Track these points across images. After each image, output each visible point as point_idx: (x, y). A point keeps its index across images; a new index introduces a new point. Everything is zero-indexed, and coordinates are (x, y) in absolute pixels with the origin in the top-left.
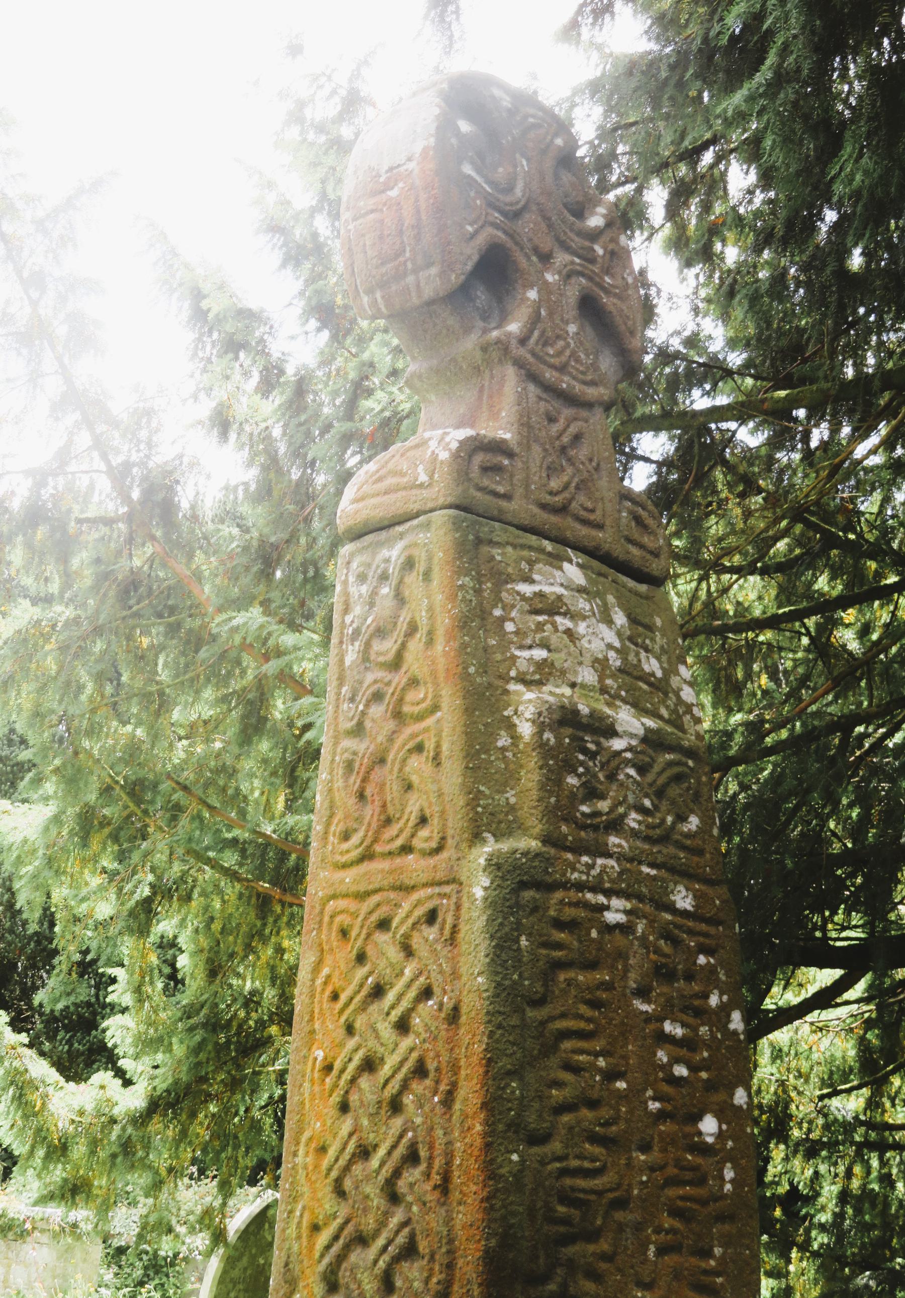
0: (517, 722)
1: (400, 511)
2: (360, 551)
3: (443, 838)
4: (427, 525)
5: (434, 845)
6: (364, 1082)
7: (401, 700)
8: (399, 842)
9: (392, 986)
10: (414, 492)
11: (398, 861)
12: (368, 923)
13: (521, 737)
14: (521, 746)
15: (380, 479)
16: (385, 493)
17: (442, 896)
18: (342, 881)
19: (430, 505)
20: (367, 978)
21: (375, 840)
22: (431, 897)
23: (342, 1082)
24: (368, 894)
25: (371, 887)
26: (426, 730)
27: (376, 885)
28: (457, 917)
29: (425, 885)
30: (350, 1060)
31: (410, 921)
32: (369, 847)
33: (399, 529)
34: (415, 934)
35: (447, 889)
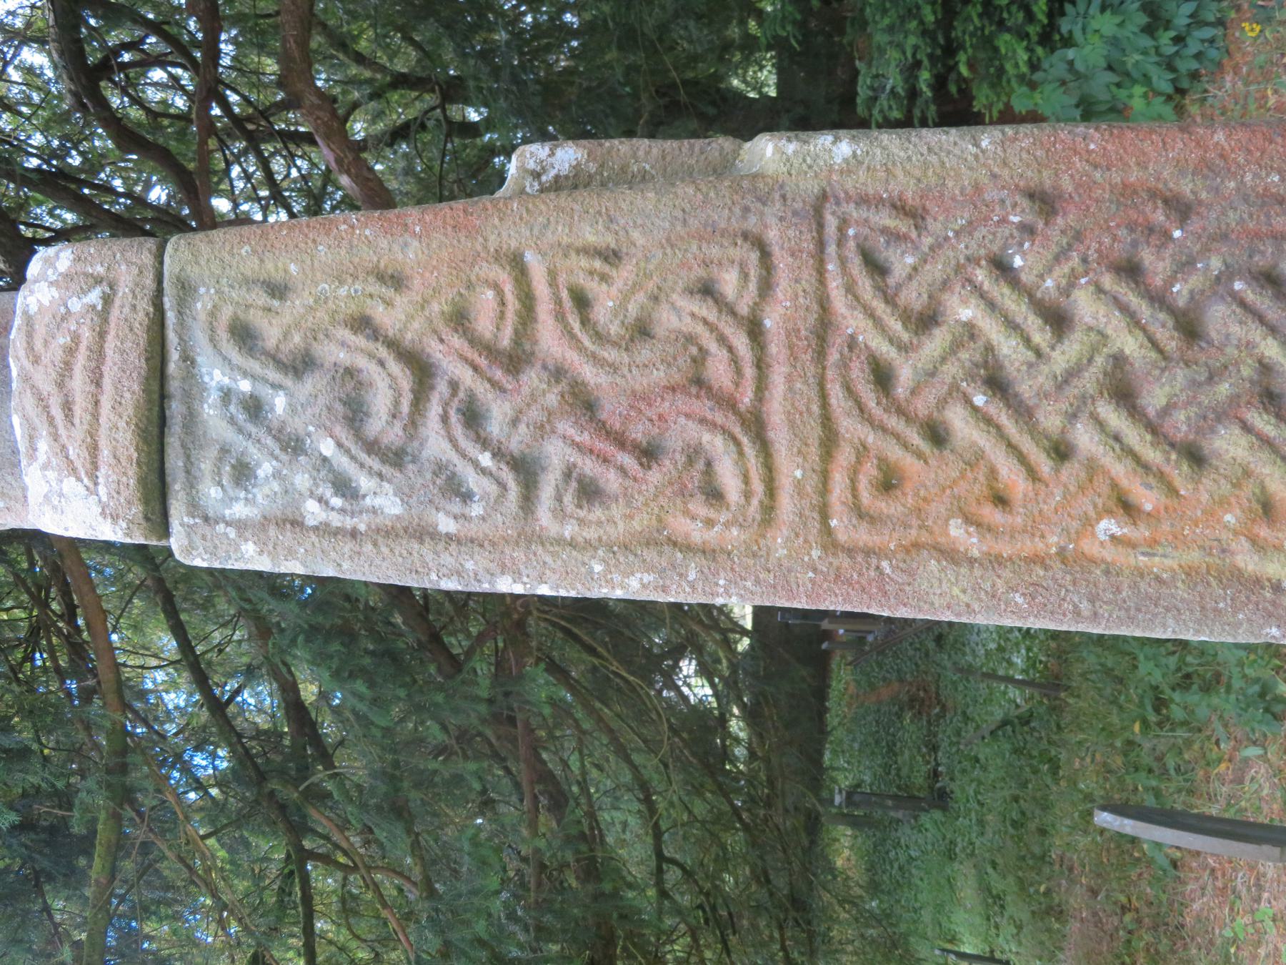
0: (552, 173)
1: (143, 338)
2: (192, 481)
3: (745, 236)
4: (186, 289)
5: (754, 256)
6: (1154, 398)
7: (489, 350)
8: (741, 342)
9: (989, 348)
10: (115, 313)
11: (775, 348)
12: (877, 412)
13: (577, 168)
14: (592, 167)
15: (67, 407)
16: (98, 384)
17: (844, 224)
18: (798, 485)
19: (149, 281)
20: (975, 409)
21: (728, 403)
22: (843, 262)
23: (1153, 455)
24: (827, 420)
25: (815, 408)
26: (552, 275)
27: (814, 394)
28: (879, 202)
29: (821, 272)
30: (1117, 438)
31: (880, 307)
32: (744, 423)
33: (174, 355)
34: (902, 300)
35: (831, 223)
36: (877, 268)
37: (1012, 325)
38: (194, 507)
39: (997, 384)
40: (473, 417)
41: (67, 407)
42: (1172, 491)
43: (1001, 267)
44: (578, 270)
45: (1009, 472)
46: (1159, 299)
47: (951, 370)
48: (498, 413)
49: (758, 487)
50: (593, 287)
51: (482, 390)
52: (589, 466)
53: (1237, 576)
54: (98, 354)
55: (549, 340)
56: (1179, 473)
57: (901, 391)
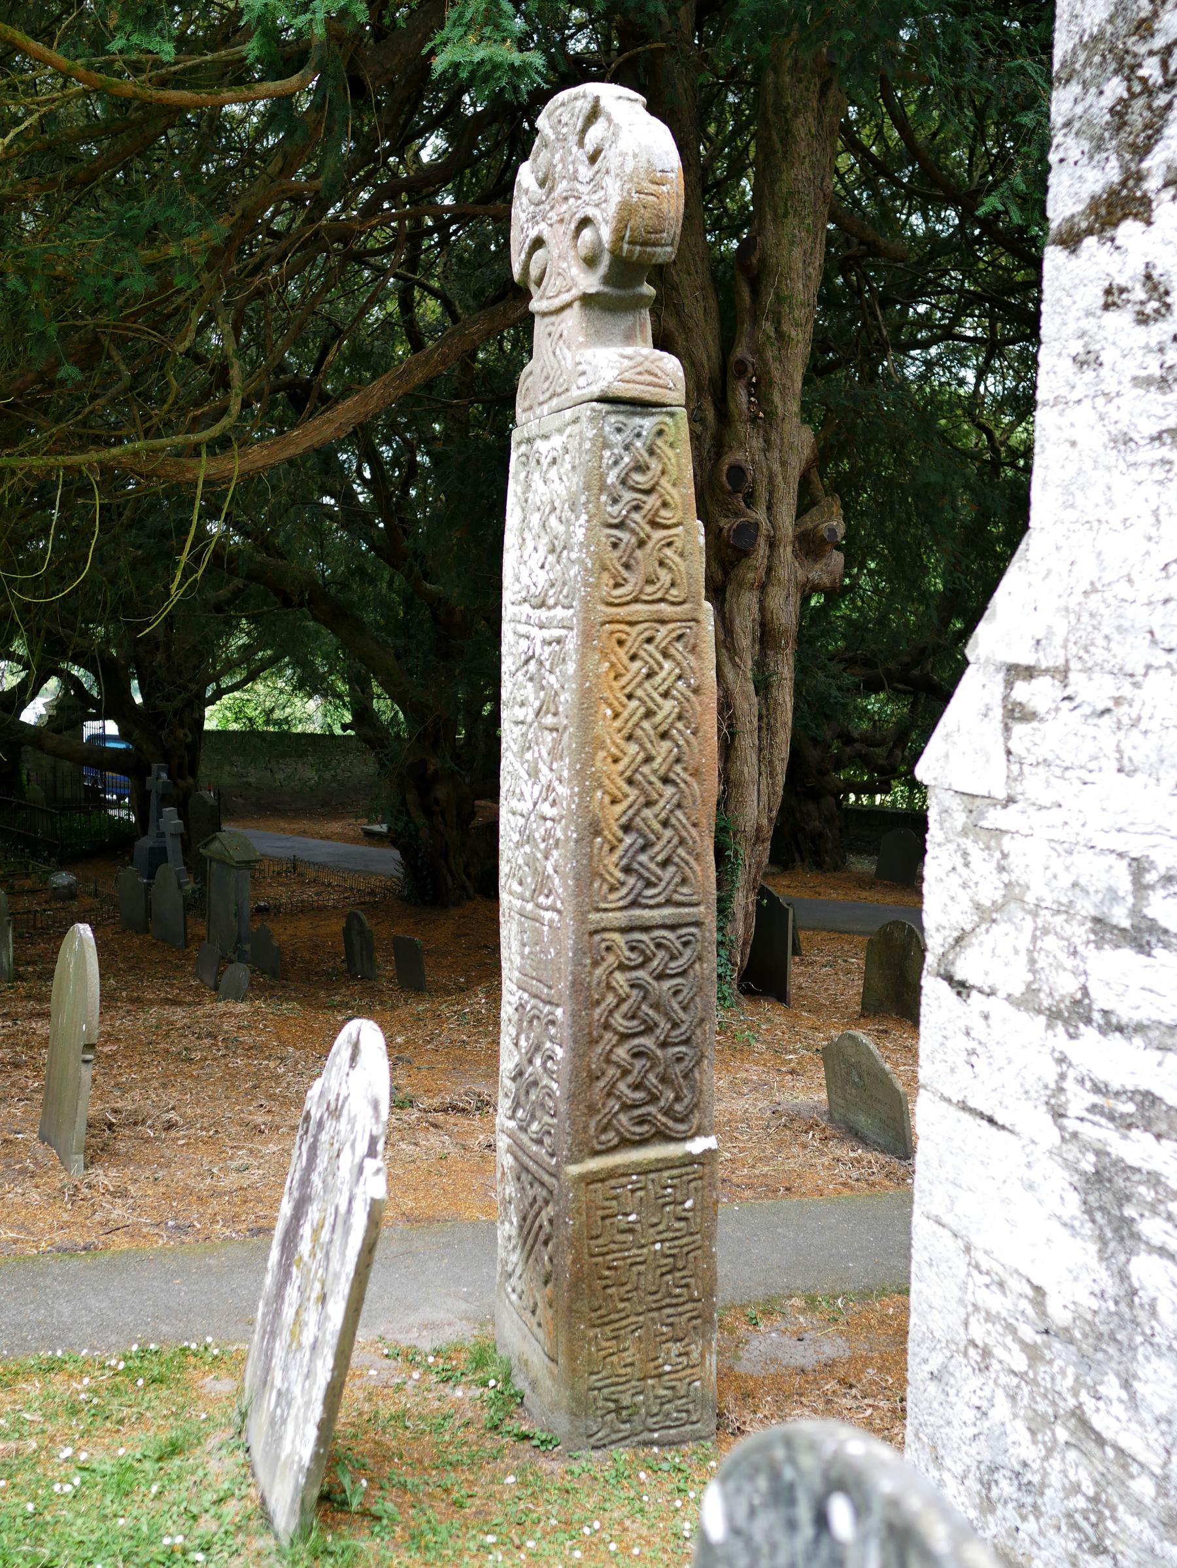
4: (672, 415)
6: (646, 724)
8: (659, 595)
15: (640, 373)
16: (649, 384)
21: (641, 592)
23: (630, 724)
36: (679, 638)
37: (664, 680)
38: (608, 413)
39: (649, 676)
40: (637, 508)
41: (640, 373)
42: (620, 731)
43: (680, 677)
44: (678, 544)
45: (623, 681)
46: (672, 725)
47: (652, 662)
48: (636, 516)
49: (617, 601)
50: (673, 548)
51: (644, 512)
52: (622, 546)
53: (595, 754)
54: (655, 385)
55: (658, 534)
56: (625, 732)
57: (646, 646)
